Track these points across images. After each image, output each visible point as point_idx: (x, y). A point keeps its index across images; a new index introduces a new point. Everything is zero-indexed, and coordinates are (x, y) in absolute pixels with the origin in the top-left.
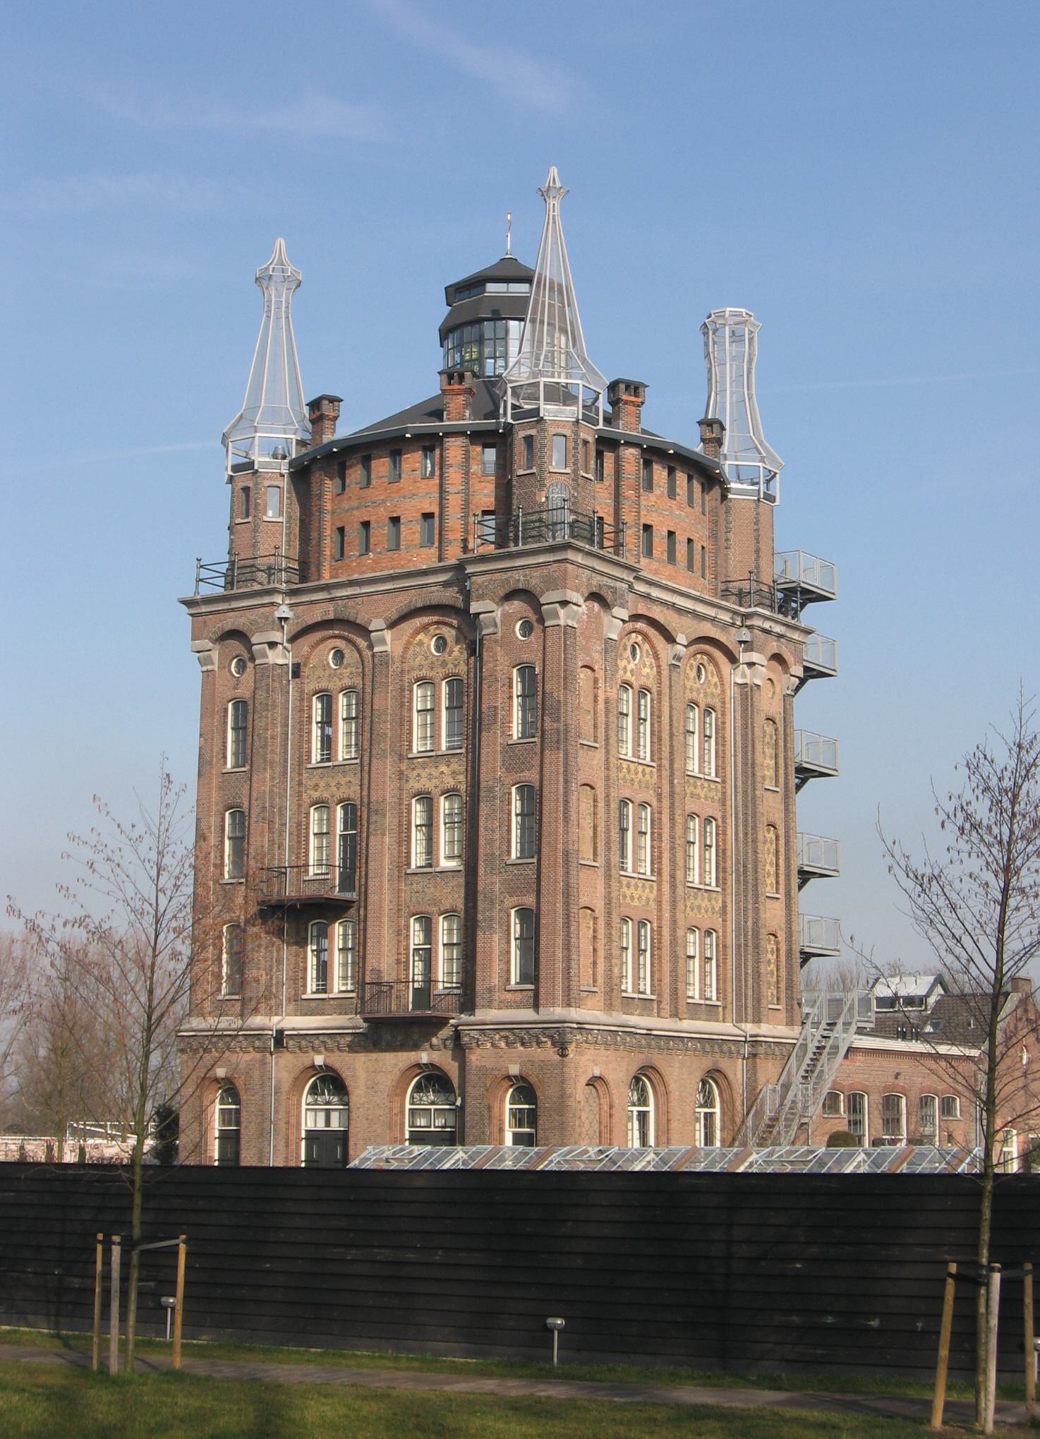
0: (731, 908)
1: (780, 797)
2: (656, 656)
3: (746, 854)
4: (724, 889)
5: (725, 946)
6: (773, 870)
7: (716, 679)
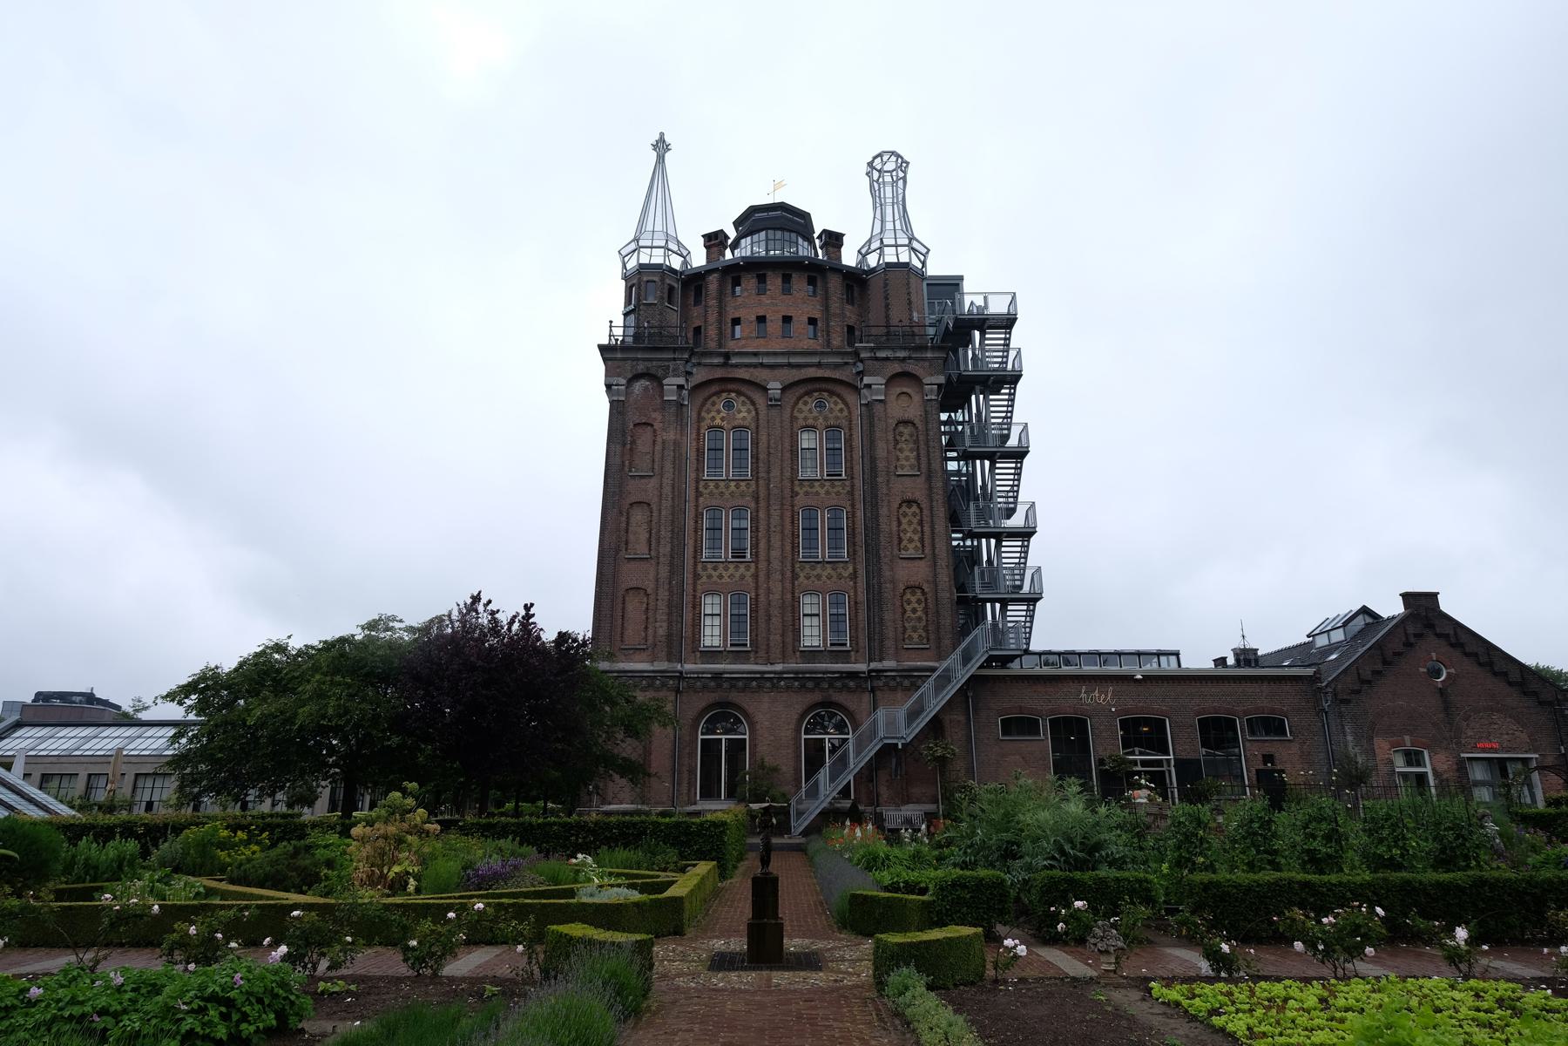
0: (862, 572)
2: (753, 403)
6: (916, 538)
7: (841, 406)
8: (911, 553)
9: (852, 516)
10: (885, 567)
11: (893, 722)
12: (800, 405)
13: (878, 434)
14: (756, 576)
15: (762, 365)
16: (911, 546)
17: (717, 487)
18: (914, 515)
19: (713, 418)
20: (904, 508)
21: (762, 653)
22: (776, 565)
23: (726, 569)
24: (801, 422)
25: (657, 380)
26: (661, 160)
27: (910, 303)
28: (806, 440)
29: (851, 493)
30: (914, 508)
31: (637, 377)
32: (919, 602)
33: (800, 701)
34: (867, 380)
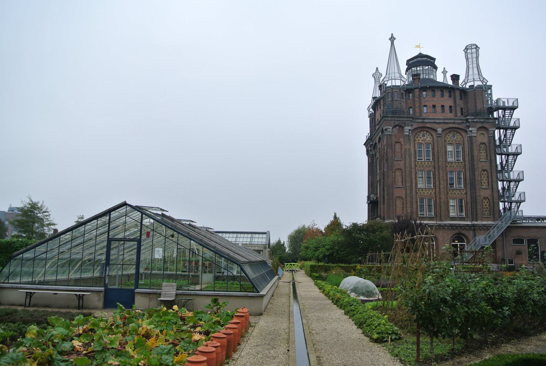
0: (469, 193)
1: (488, 164)
2: (432, 135)
6: (486, 182)
7: (460, 137)
8: (485, 187)
9: (465, 174)
10: (477, 191)
11: (482, 240)
12: (447, 136)
13: (474, 148)
14: (435, 193)
15: (435, 122)
16: (485, 185)
17: (421, 163)
18: (486, 174)
19: (419, 140)
20: (482, 172)
21: (438, 218)
22: (442, 190)
23: (426, 191)
24: (448, 142)
25: (401, 127)
26: (392, 43)
27: (483, 102)
28: (450, 148)
29: (465, 166)
30: (486, 172)
31: (395, 126)
32: (487, 202)
33: (451, 233)
34: (470, 129)
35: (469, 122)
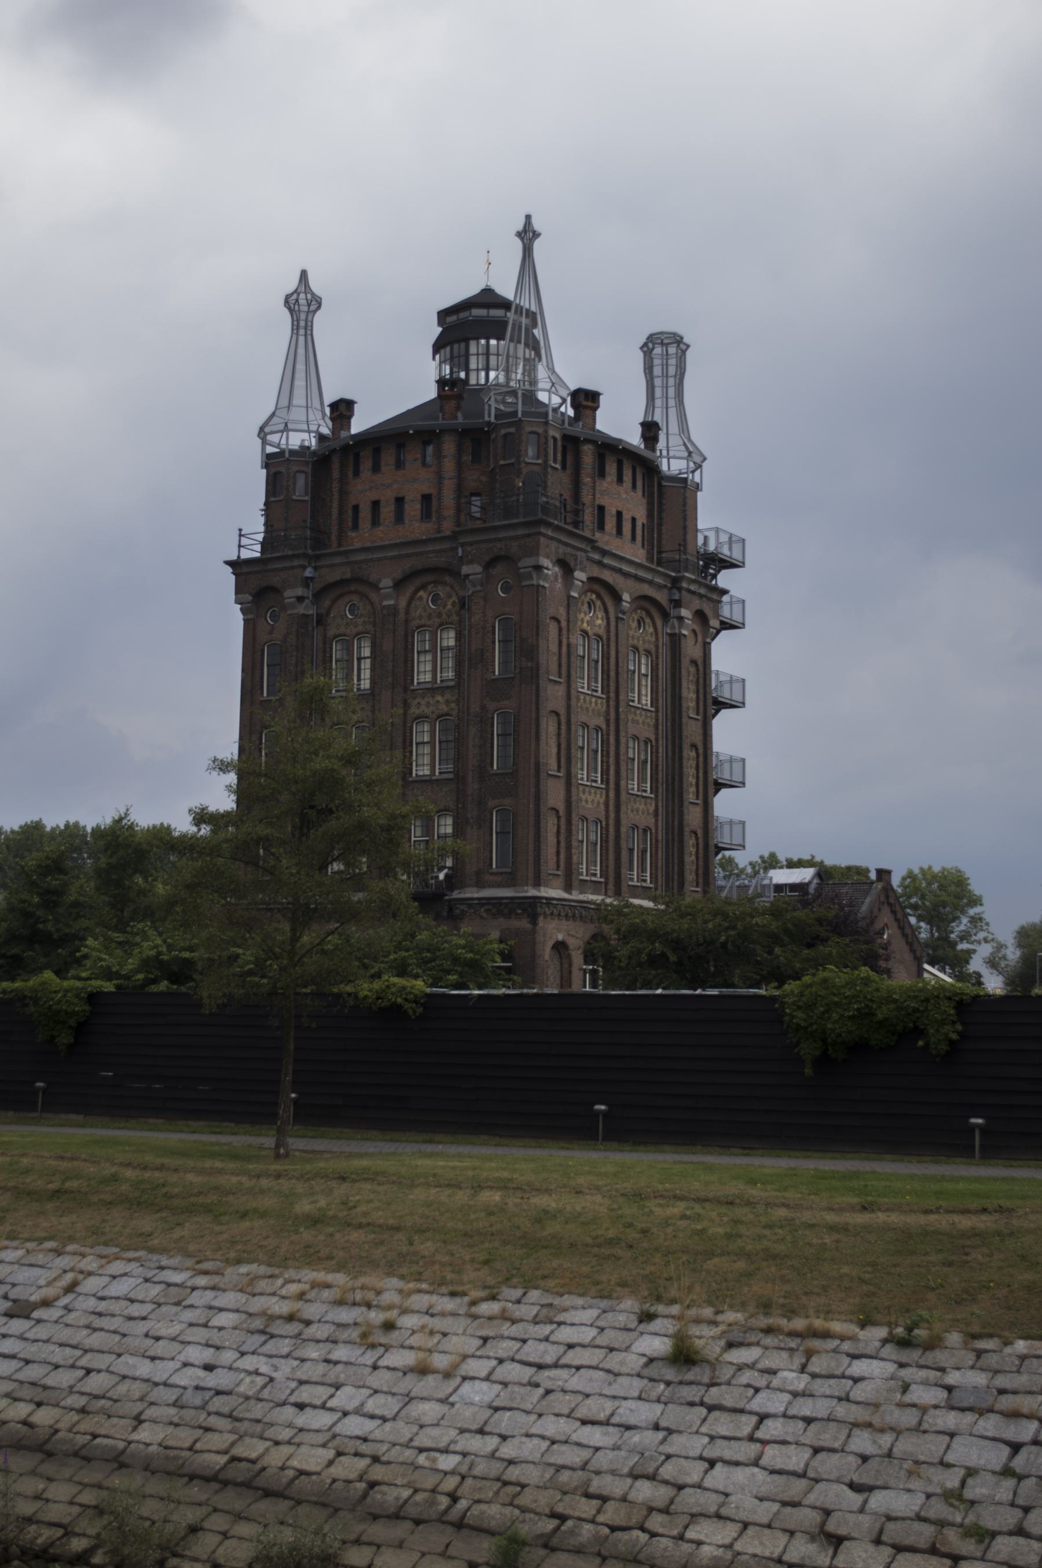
1: (700, 724)
3: (673, 768)
4: (657, 796)
5: (657, 841)
6: (694, 781)
7: (651, 630)
35: (680, 589)
